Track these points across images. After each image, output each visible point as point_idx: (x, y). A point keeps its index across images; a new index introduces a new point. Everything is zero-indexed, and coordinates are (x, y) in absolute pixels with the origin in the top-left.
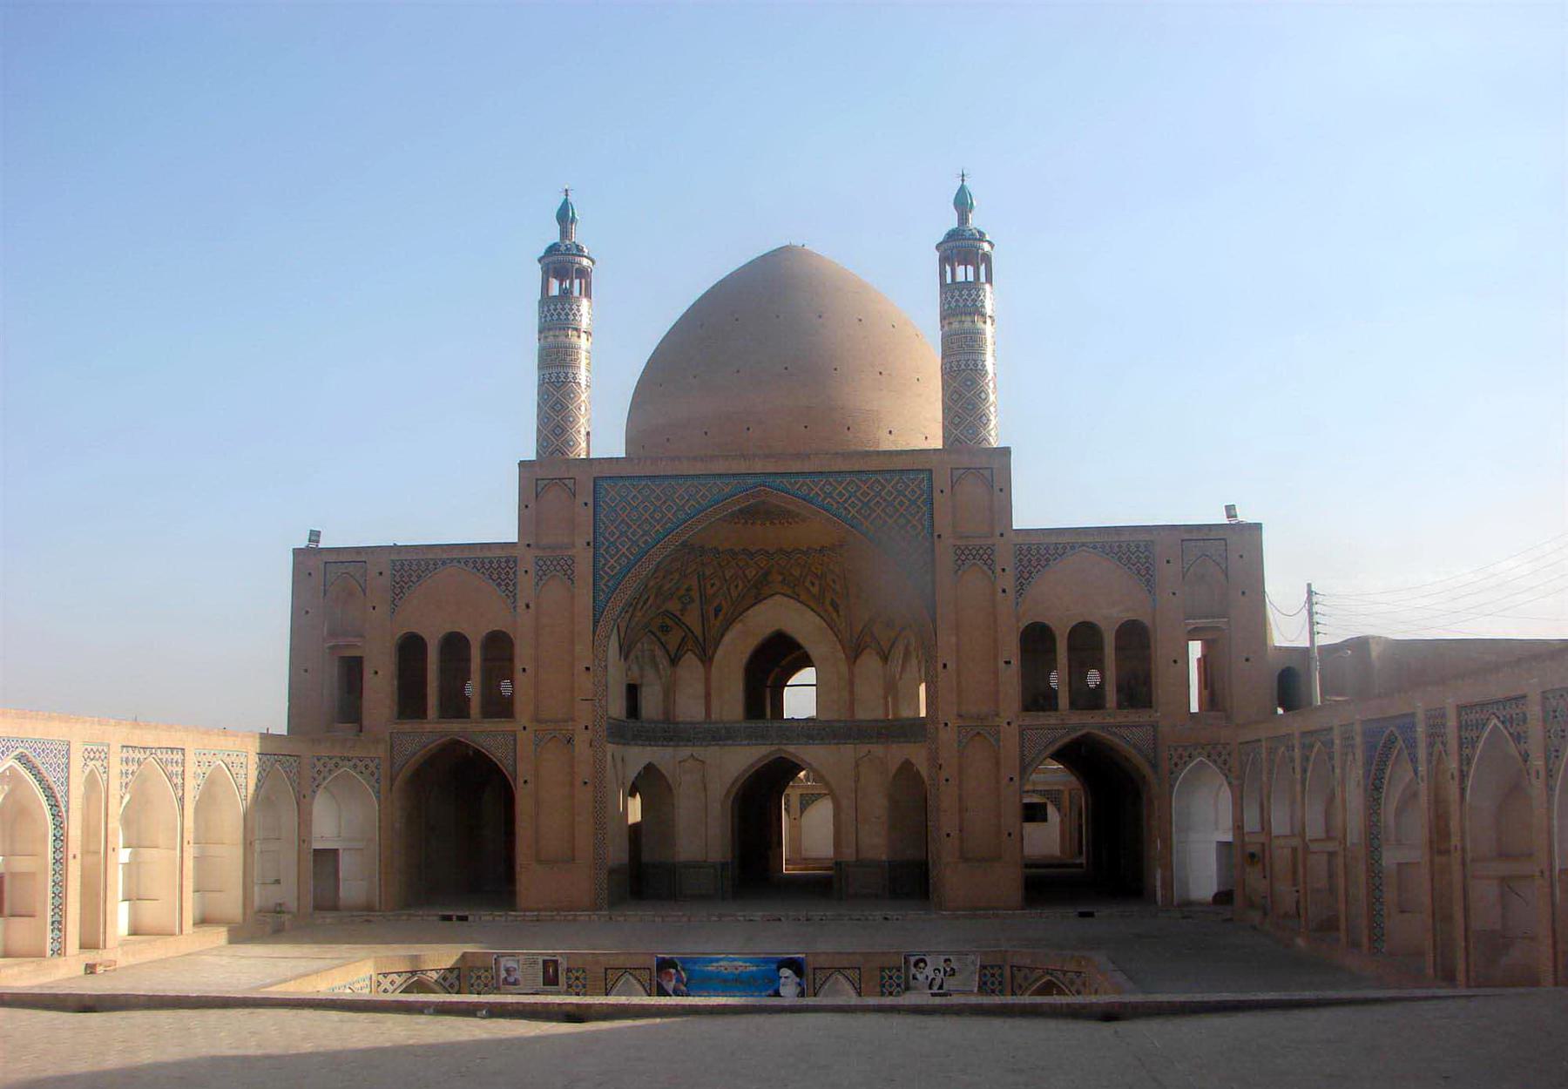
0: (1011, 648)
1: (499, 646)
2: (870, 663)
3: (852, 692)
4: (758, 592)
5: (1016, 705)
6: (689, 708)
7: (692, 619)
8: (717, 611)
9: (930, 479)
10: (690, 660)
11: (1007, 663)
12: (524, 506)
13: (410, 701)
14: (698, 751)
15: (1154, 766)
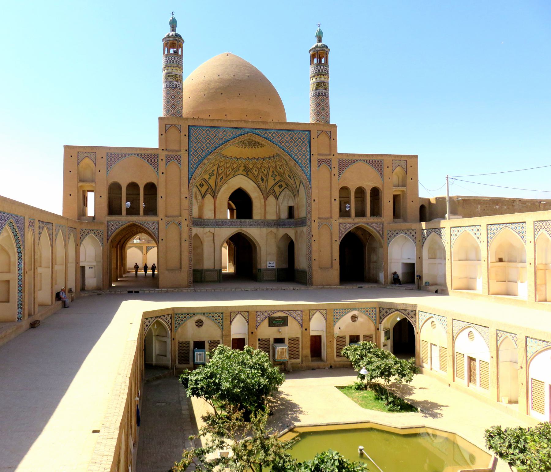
0: (336, 195)
1: (151, 188)
2: (271, 199)
3: (265, 210)
4: (235, 173)
5: (338, 215)
6: (208, 214)
7: (212, 182)
8: (221, 179)
9: (310, 134)
10: (209, 197)
11: (335, 200)
12: (161, 135)
13: (114, 209)
14: (212, 230)
15: (382, 237)
